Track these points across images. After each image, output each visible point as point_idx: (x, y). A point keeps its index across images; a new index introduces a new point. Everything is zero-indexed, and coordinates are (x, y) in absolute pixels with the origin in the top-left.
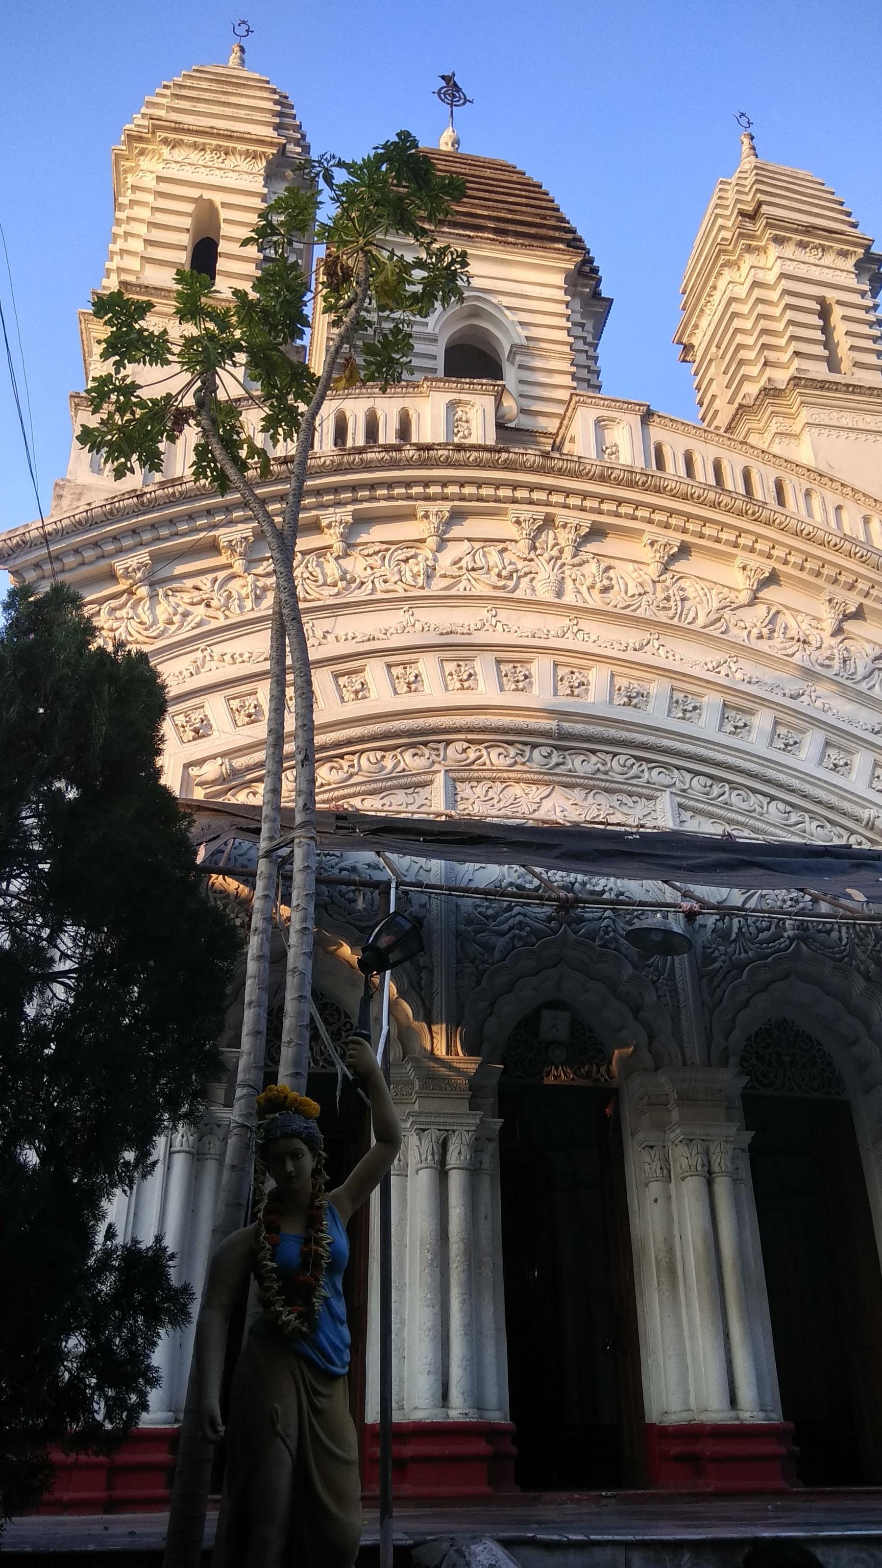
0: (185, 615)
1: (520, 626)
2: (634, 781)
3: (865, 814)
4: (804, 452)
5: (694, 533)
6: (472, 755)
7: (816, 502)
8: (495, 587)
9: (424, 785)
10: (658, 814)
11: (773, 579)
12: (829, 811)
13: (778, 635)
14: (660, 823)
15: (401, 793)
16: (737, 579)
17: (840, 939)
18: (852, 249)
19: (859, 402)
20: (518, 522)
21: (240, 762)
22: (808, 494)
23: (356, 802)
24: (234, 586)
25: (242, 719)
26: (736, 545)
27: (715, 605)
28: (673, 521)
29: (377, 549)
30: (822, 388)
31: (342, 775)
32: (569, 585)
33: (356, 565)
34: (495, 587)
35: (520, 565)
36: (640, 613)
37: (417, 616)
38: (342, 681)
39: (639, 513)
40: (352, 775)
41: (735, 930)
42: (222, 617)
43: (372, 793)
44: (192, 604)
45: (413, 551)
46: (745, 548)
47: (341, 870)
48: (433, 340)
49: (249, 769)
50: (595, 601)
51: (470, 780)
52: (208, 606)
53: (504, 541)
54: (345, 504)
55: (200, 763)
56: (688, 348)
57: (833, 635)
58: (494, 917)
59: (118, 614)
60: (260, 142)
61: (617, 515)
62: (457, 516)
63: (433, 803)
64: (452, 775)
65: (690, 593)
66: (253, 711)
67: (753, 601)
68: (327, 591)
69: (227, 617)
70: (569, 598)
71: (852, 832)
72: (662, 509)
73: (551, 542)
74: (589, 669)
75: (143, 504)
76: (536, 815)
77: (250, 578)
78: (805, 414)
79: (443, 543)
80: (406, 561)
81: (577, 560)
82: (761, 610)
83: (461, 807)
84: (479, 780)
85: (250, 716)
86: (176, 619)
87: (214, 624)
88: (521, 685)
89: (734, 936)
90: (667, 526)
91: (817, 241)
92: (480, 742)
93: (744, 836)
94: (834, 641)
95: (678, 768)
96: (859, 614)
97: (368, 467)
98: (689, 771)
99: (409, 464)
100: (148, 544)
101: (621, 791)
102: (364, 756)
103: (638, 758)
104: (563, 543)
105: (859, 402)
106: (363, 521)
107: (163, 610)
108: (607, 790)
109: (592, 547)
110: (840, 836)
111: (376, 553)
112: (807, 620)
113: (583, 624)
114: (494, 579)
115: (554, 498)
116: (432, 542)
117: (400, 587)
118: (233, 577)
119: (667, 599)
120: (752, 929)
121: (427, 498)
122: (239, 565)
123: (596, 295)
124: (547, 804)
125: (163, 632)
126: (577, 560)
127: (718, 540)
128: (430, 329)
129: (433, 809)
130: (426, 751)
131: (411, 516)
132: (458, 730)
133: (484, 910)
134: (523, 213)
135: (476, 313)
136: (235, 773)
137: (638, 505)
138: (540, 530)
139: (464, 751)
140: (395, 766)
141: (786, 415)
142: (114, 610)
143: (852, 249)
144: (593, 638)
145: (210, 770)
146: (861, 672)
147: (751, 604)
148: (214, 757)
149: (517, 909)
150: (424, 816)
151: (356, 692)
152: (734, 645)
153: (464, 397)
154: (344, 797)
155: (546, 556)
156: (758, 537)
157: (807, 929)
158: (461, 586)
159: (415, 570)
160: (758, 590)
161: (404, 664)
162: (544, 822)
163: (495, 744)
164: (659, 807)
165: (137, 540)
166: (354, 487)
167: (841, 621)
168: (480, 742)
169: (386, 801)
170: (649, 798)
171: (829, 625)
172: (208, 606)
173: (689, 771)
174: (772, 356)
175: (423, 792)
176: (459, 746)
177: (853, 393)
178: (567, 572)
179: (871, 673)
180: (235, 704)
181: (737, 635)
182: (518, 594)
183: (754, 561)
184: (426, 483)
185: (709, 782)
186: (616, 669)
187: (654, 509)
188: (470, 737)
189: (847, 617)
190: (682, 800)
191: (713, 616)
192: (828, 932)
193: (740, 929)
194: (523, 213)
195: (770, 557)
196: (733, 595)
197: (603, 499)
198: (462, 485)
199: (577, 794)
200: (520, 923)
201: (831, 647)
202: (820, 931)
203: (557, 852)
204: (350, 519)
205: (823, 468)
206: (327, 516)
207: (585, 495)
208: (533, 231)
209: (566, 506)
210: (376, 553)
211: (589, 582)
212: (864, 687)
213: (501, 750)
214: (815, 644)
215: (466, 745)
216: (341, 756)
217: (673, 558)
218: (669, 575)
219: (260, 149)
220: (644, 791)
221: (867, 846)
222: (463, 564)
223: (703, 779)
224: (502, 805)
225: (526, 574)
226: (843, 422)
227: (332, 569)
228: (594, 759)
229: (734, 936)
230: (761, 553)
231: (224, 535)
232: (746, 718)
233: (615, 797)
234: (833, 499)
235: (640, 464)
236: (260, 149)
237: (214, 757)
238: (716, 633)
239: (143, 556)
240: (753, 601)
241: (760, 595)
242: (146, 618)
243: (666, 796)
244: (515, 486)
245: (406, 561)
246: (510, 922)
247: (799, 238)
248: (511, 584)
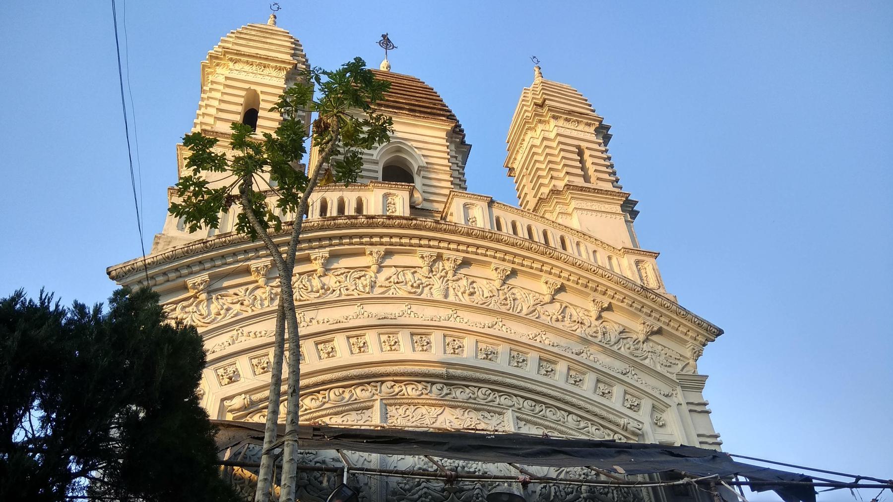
0: (228, 310)
1: (424, 314)
2: (491, 404)
3: (622, 422)
4: (574, 222)
5: (518, 264)
6: (397, 389)
7: (582, 248)
8: (410, 293)
9: (368, 408)
10: (506, 423)
11: (562, 289)
12: (602, 421)
14: (506, 429)
15: (354, 413)
16: (542, 288)
17: (613, 498)
20: (422, 257)
21: (255, 397)
22: (578, 244)
23: (326, 420)
24: (258, 293)
25: (259, 370)
26: (541, 271)
27: (532, 303)
28: (507, 257)
29: (342, 271)
31: (318, 403)
32: (451, 291)
33: (330, 281)
34: (410, 293)
35: (424, 280)
36: (490, 307)
37: (365, 309)
38: (320, 347)
39: (488, 253)
40: (324, 403)
41: (553, 494)
42: (250, 311)
44: (233, 303)
45: (363, 273)
46: (546, 272)
47: (316, 462)
49: (261, 401)
50: (466, 300)
51: (395, 404)
52: (242, 304)
53: (415, 267)
54: (325, 247)
55: (231, 398)
56: (511, 170)
57: (597, 319)
58: (409, 490)
59: (187, 310)
60: (284, 62)
61: (477, 254)
62: (389, 254)
63: (373, 420)
64: (384, 401)
65: (518, 296)
66: (265, 365)
67: (553, 301)
68: (313, 295)
69: (253, 310)
70: (452, 298)
71: (616, 432)
72: (501, 251)
73: (441, 268)
74: (463, 338)
75: (206, 247)
76: (434, 425)
77: (268, 288)
78: (574, 204)
79: (380, 268)
80: (359, 278)
81: (455, 278)
82: (557, 305)
83: (390, 421)
84: (401, 405)
85: (263, 368)
86: (222, 312)
87: (245, 315)
88: (425, 348)
89: (552, 498)
90: (504, 260)
92: (401, 382)
93: (555, 435)
94: (598, 323)
95: (516, 396)
96: (609, 308)
97: (338, 227)
98: (522, 397)
99: (362, 226)
100: (208, 269)
101: (484, 410)
102: (332, 391)
104: (447, 268)
106: (335, 256)
107: (214, 307)
108: (476, 410)
109: (463, 271)
110: (609, 435)
111: (342, 274)
112: (582, 311)
113: (460, 313)
114: (409, 288)
115: (442, 245)
116: (374, 268)
117: (355, 293)
119: (506, 299)
120: (563, 493)
121: (372, 244)
122: (262, 281)
123: (463, 142)
124: (441, 418)
125: (214, 320)
126: (455, 278)
127: (532, 268)
128: (374, 158)
129: (373, 423)
130: (369, 388)
131: (363, 254)
132: (388, 375)
133: (403, 485)
134: (423, 102)
135: (400, 150)
136: (252, 403)
137: (488, 249)
138: (435, 261)
139: (392, 387)
140: (351, 397)
141: (564, 204)
142: (184, 307)
144: (466, 320)
145: (237, 402)
146: (613, 340)
148: (240, 394)
149: (424, 484)
150: (368, 428)
151: (329, 353)
152: (543, 325)
153: (391, 191)
154: (319, 417)
155: (438, 275)
156: (553, 266)
157: (594, 492)
158: (390, 292)
159: (365, 283)
160: (554, 295)
161: (357, 336)
162: (439, 429)
163: (410, 383)
164: (505, 419)
165: (202, 267)
166: (330, 238)
167: (600, 312)
168: (401, 382)
169: (345, 419)
170: (500, 414)
171: (594, 314)
172: (242, 304)
173: (522, 397)
174: (555, 174)
175: (367, 413)
176: (389, 384)
178: (450, 285)
180: (255, 361)
181: (545, 319)
182: (423, 296)
183: (551, 279)
184: (371, 236)
185: (534, 404)
187: (497, 251)
188: (395, 378)
189: (603, 310)
190: (519, 415)
191: (531, 309)
192: (606, 494)
193: (555, 493)
194: (423, 102)
195: (560, 277)
196: (541, 297)
197: (469, 245)
198: (391, 237)
199: (458, 412)
200: (425, 493)
201: (596, 326)
202: (601, 493)
203: (446, 447)
204: (327, 255)
205: (585, 231)
206: (314, 254)
207: (459, 243)
208: (429, 110)
209: (449, 249)
210: (342, 274)
211: (462, 290)
212: (615, 348)
213: (413, 386)
214: (587, 324)
215: (393, 383)
216: (318, 392)
217: (508, 277)
218: (506, 286)
219: (283, 66)
220: (497, 410)
221: (624, 440)
222: (392, 280)
223: (530, 402)
224: (414, 419)
225: (427, 285)
226: (594, 208)
227: (316, 283)
228: (467, 391)
229: (552, 498)
230: (555, 275)
231: (254, 264)
232: (553, 366)
233: (480, 413)
234: (592, 247)
235: (488, 227)
236: (283, 66)
237: (240, 394)
238: (533, 318)
239: (205, 276)
240: (553, 301)
241: (556, 297)
242: (204, 311)
243: (510, 412)
244: (420, 238)
245: (359, 278)
246: (420, 493)
248: (419, 291)
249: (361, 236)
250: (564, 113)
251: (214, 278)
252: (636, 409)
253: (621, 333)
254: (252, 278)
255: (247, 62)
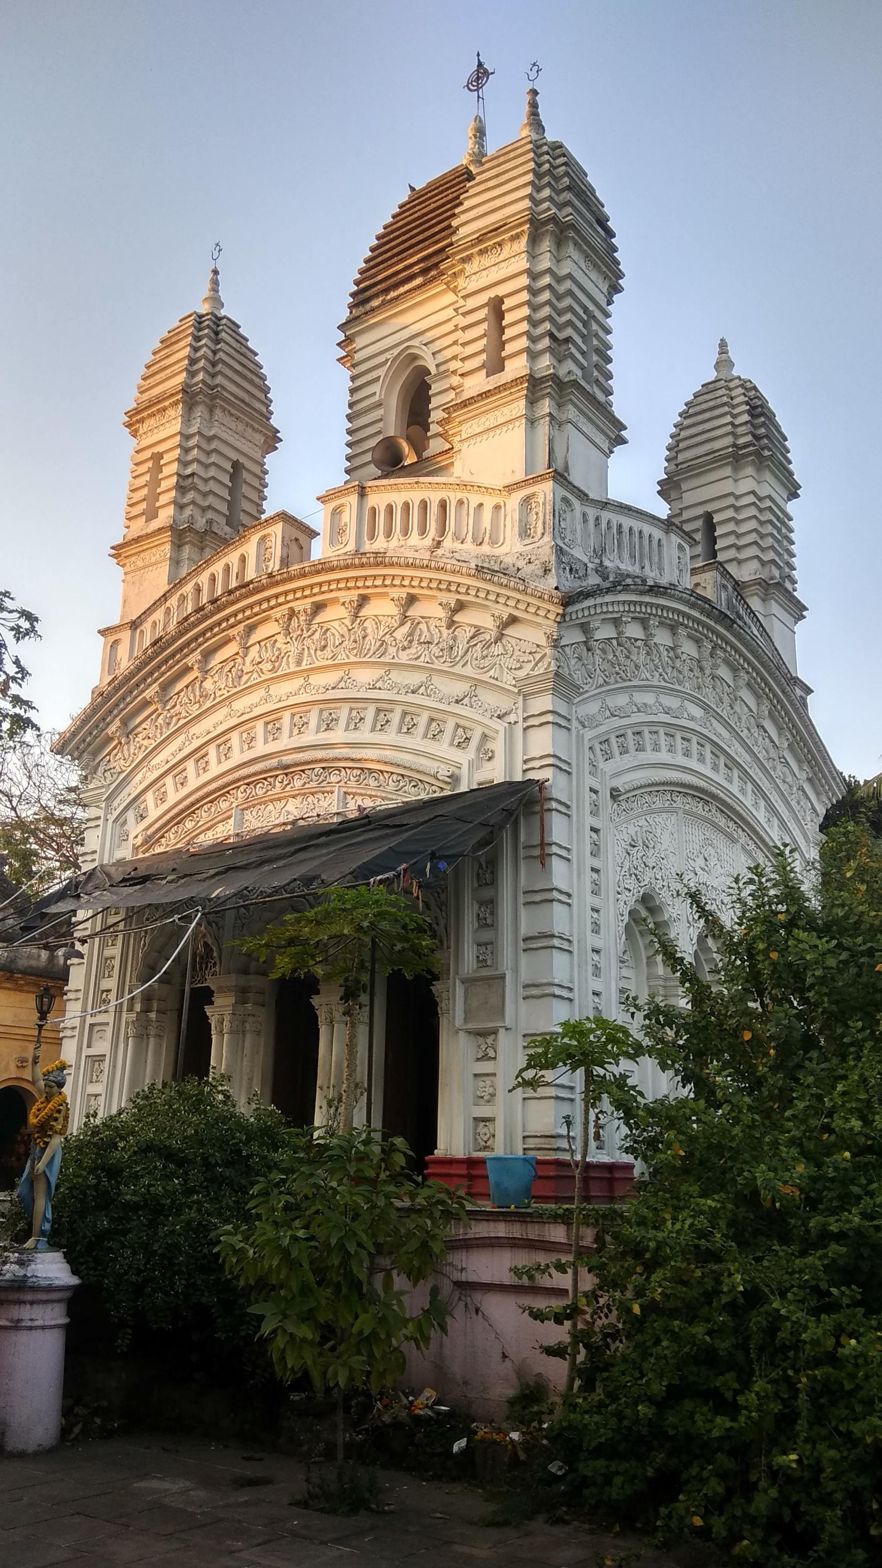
13: (415, 643)
18: (519, 230)
19: (495, 401)
20: (277, 621)
21: (149, 832)
30: (466, 406)
43: (208, 829)
48: (379, 405)
49: (155, 833)
51: (249, 807)
62: (251, 629)
82: (406, 629)
84: (254, 806)
91: (491, 243)
99: (213, 614)
103: (324, 768)
105: (495, 401)
106: (208, 655)
115: (290, 597)
118: (160, 715)
121: (232, 626)
128: (376, 398)
131: (227, 641)
132: (238, 780)
143: (519, 230)
147: (402, 624)
160: (405, 611)
161: (225, 743)
166: (195, 638)
177: (487, 397)
179: (467, 651)
186: (322, 706)
189: (455, 611)
190: (345, 790)
217: (360, 606)
220: (328, 789)
231: (148, 694)
239: (117, 723)
244: (268, 599)
247: (477, 249)
249: (219, 624)
250: (473, 246)
251: (125, 723)
252: (464, 745)
253: (472, 638)
254: (153, 708)
255: (150, 416)
